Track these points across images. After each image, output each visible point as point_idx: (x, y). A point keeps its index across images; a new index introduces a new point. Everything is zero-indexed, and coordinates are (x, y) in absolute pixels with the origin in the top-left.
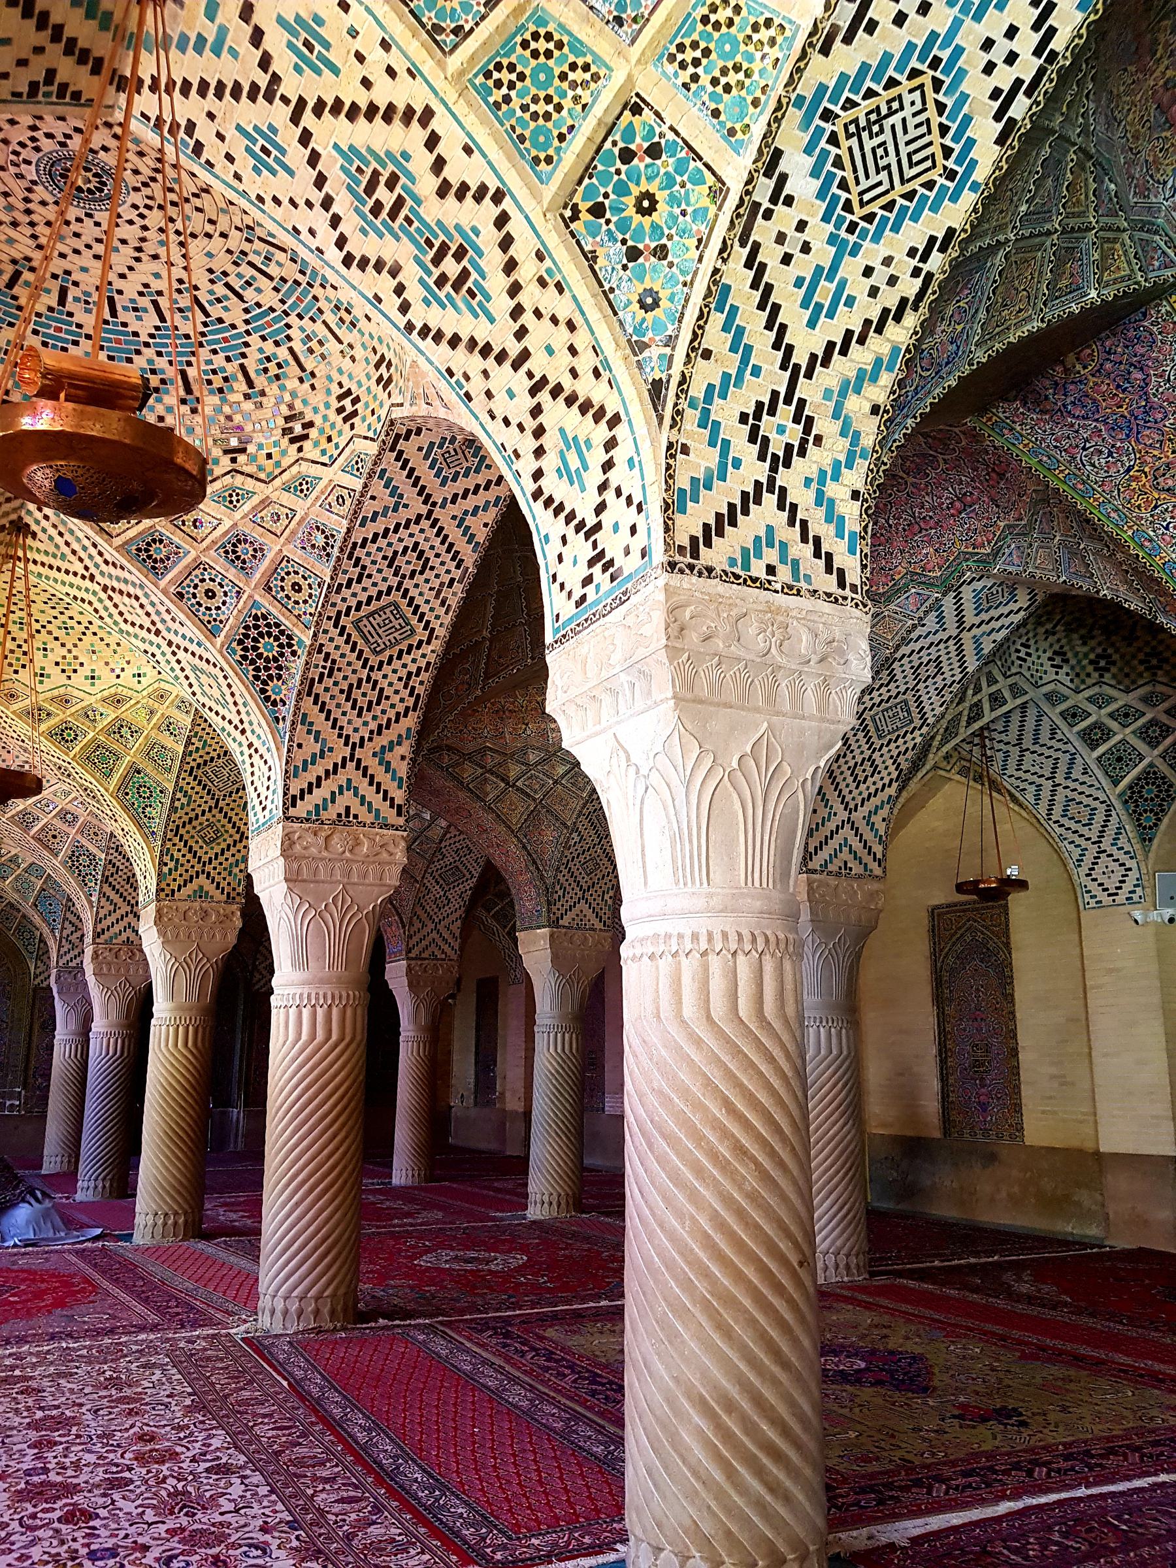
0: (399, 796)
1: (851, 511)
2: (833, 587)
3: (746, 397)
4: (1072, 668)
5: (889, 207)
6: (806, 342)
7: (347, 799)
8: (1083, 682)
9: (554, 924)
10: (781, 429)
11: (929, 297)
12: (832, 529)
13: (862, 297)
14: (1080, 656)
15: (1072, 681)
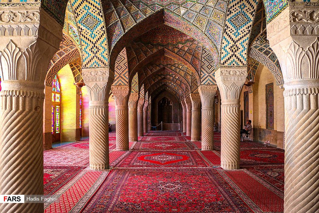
0: (128, 81)
1: (106, 56)
2: (104, 66)
3: (90, 47)
4: (260, 41)
5: (94, 26)
6: (94, 41)
7: (120, 82)
8: (263, 43)
9: (192, 93)
10: (95, 50)
11: (105, 32)
12: (104, 59)
13: (98, 35)
14: (261, 38)
15: (260, 43)
